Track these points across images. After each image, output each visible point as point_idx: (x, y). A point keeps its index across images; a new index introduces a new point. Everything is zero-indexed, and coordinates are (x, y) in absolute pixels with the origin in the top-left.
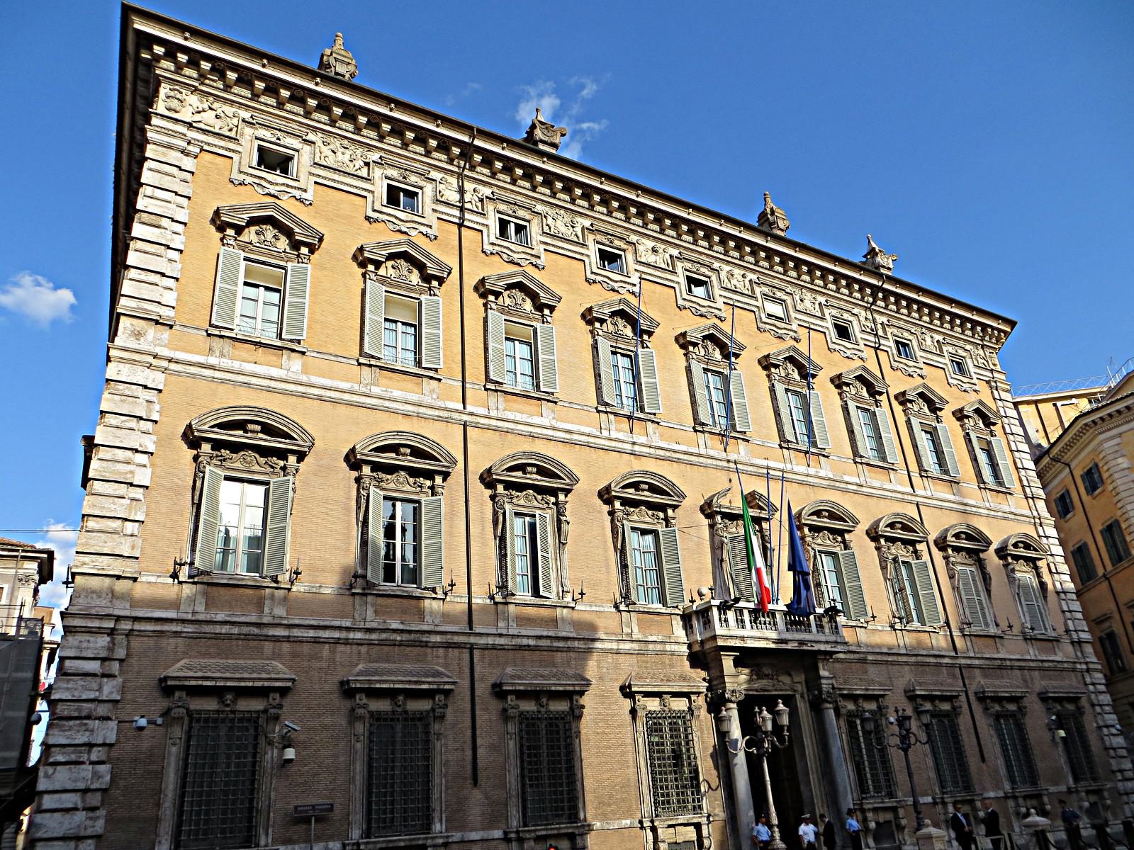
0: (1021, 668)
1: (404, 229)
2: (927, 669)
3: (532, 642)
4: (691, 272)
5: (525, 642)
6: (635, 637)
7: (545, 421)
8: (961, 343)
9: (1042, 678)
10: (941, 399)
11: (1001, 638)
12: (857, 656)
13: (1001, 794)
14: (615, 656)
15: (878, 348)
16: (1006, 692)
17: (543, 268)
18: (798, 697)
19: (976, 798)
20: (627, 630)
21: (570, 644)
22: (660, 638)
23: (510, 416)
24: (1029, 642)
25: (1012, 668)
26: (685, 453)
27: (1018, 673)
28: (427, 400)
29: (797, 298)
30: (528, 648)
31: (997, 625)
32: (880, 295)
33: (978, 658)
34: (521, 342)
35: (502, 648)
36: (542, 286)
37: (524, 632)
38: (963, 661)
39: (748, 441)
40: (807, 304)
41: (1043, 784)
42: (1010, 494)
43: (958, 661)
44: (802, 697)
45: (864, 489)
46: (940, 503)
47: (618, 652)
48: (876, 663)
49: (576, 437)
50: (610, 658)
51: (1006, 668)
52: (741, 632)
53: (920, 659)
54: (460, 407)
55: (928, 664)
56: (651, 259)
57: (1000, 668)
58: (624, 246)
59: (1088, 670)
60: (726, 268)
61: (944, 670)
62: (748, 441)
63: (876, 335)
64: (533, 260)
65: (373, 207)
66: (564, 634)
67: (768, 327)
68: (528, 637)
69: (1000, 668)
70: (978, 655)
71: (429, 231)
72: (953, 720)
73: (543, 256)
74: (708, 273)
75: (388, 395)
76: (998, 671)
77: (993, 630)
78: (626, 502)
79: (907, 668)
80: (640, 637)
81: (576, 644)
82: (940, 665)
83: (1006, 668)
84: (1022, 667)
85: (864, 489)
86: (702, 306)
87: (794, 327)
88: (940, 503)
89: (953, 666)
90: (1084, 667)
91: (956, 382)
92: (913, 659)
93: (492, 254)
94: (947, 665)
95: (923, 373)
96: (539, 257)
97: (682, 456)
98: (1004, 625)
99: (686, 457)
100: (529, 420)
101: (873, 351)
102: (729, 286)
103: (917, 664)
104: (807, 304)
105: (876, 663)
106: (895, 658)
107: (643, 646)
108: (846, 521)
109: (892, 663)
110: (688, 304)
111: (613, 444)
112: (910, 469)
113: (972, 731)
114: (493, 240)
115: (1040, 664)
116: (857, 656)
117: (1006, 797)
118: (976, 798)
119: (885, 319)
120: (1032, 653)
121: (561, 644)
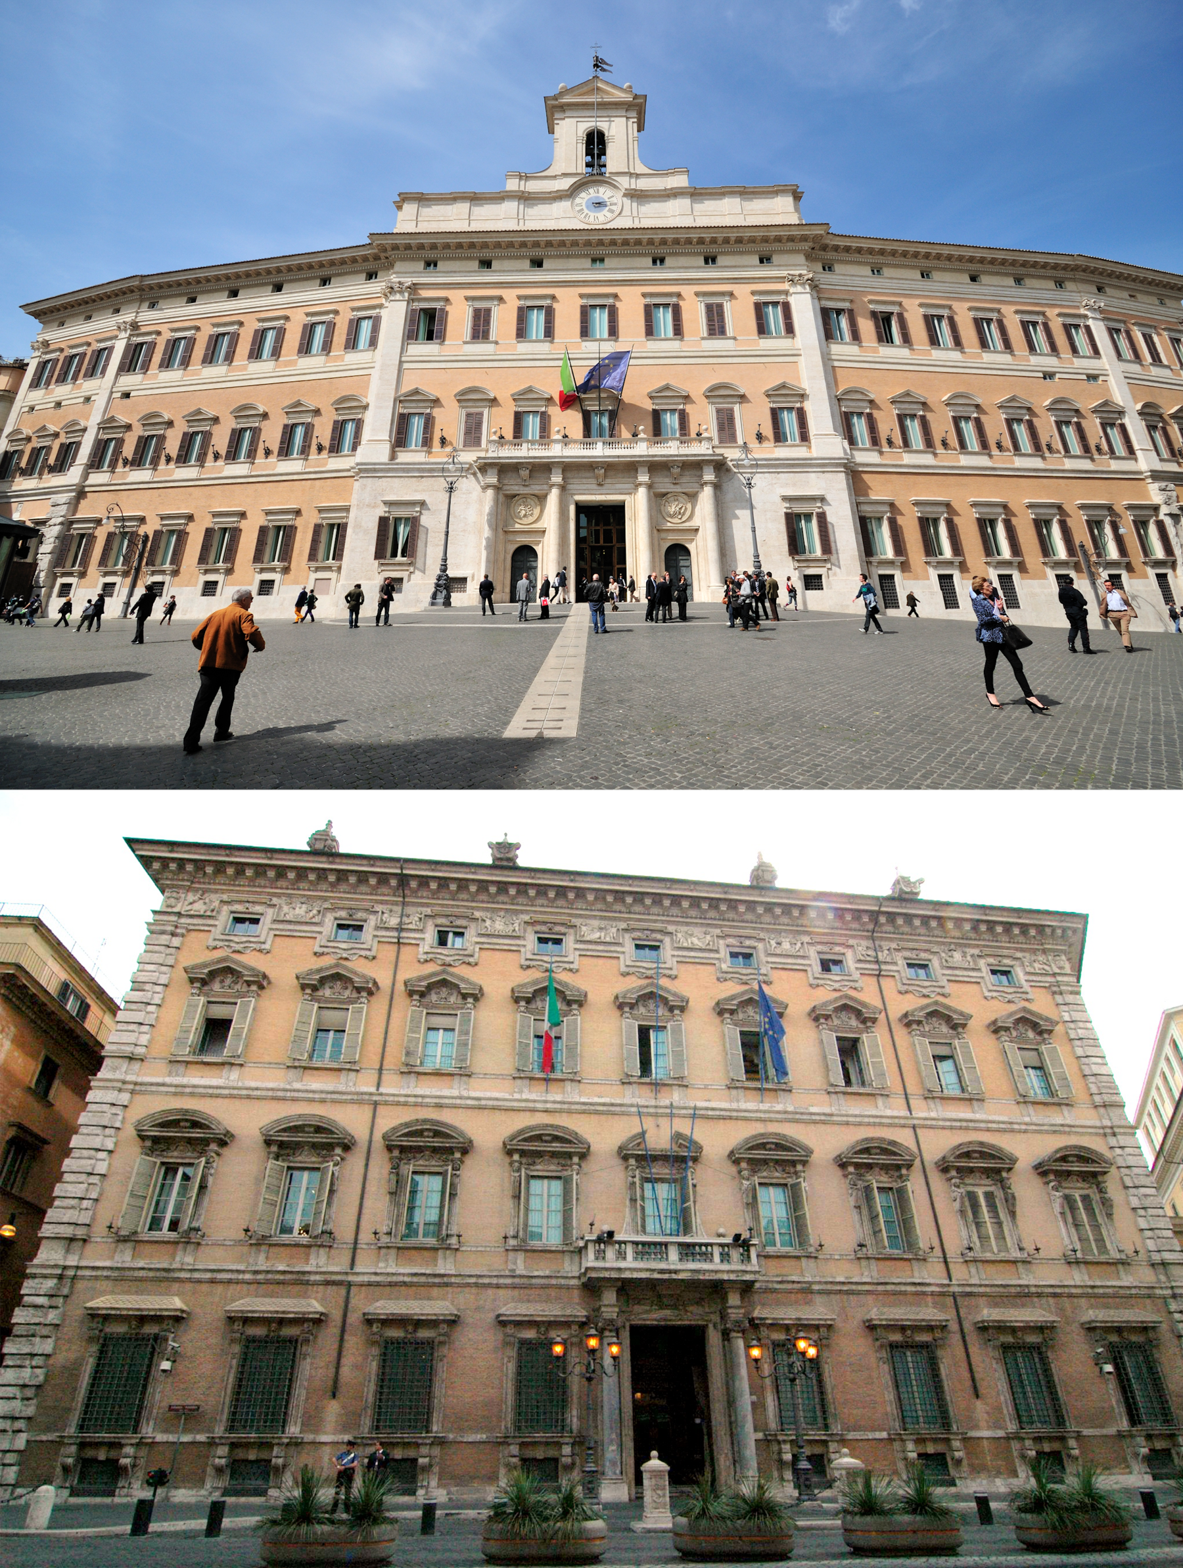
0: (1055, 1295)
1: (345, 955)
2: (901, 1297)
3: (406, 1279)
4: (640, 939)
5: (401, 1279)
6: (518, 1272)
7: (455, 1093)
8: (1005, 952)
9: (1092, 1307)
10: (961, 1014)
11: (1029, 1262)
12: (796, 1286)
13: (1000, 1433)
14: (495, 1290)
15: (879, 975)
17: (476, 964)
18: (711, 1326)
19: (952, 1437)
20: (511, 1266)
21: (445, 1280)
22: (547, 1273)
23: (419, 1091)
24: (1074, 1266)
25: (1039, 1295)
26: (604, 1105)
27: (1051, 1300)
28: (342, 1088)
29: (773, 943)
30: (405, 1284)
31: (1021, 1249)
32: (883, 919)
33: (986, 1286)
34: (445, 1030)
35: (378, 1284)
36: (462, 979)
37: (402, 1271)
38: (957, 1289)
39: (687, 1086)
40: (786, 946)
41: (1072, 1426)
42: (1067, 1105)
43: (951, 1289)
44: (715, 1326)
45: (835, 1118)
46: (948, 1123)
47: (498, 1286)
48: (820, 1292)
49: (483, 1102)
50: (490, 1292)
51: (1028, 1295)
52: (622, 1265)
53: (889, 1288)
54: (373, 1090)
55: (904, 1293)
56: (595, 936)
57: (1018, 1295)
58: (563, 929)
59: (1174, 1296)
60: (684, 929)
61: (929, 1298)
62: (687, 1086)
63: (877, 962)
64: (467, 959)
66: (442, 1272)
67: (730, 976)
68: (404, 1275)
70: (983, 1282)
71: (368, 953)
72: (933, 1353)
73: (476, 955)
74: (659, 936)
75: (308, 1088)
77: (1015, 1254)
78: (523, 1153)
79: (870, 1298)
80: (524, 1273)
81: (453, 1280)
82: (924, 1293)
83: (1028, 1295)
84: (1056, 1294)
85: (835, 1118)
87: (763, 971)
88: (948, 1123)
89: (942, 1294)
90: (1169, 1292)
91: (995, 994)
92: (880, 1288)
93: (426, 961)
94: (932, 1293)
95: (946, 991)
96: (472, 956)
97: (601, 1108)
98: (1030, 1248)
99: (605, 1108)
100: (438, 1093)
101: (875, 979)
102: (685, 945)
103: (886, 1293)
104: (786, 946)
105: (820, 1292)
106: (854, 1287)
107: (525, 1281)
108: (796, 1151)
109: (848, 1293)
110: (632, 970)
111: (523, 1104)
112: (909, 1091)
113: (964, 1365)
115: (1090, 1291)
116: (799, 1286)
117: (1008, 1438)
118: (952, 1437)
119: (894, 945)
121: (437, 1280)
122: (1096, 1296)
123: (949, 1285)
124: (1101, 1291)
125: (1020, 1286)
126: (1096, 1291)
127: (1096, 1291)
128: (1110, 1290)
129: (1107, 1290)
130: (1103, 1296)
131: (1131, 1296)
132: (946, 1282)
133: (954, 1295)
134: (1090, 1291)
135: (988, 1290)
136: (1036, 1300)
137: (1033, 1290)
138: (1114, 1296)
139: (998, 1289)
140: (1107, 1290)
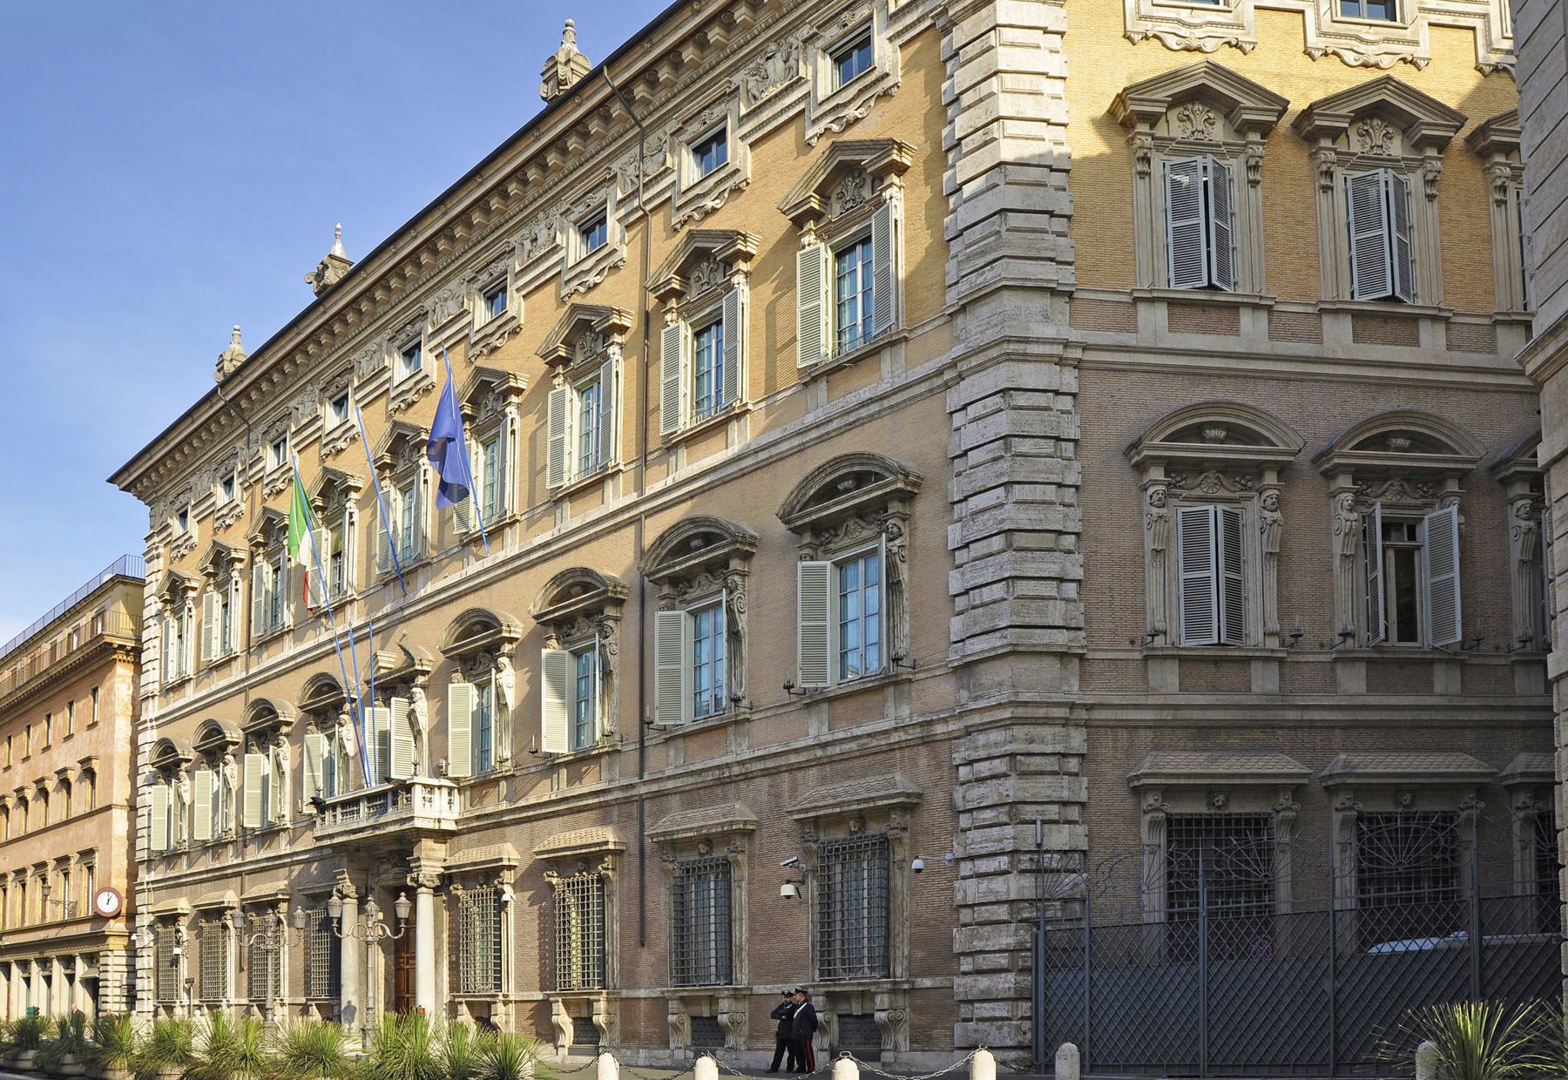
0: (767, 773)
9: (823, 780)
16: (691, 829)
25: (748, 777)
51: (733, 780)
57: (721, 783)
65: (1318, 28)
69: (721, 783)
76: (719, 791)
83: (733, 780)
86: (1367, 42)
89: (628, 801)
94: (618, 802)
114: (1326, 25)
115: (819, 753)
120: (815, 729)
122: (832, 761)
123: (632, 786)
124: (837, 750)
125: (718, 767)
126: (830, 751)
127: (830, 751)
128: (853, 746)
129: (846, 747)
130: (844, 758)
131: (891, 749)
132: (636, 780)
133: (642, 800)
134: (819, 753)
135: (678, 783)
136: (743, 785)
137: (736, 770)
138: (864, 754)
139: (691, 780)
140: (846, 747)
